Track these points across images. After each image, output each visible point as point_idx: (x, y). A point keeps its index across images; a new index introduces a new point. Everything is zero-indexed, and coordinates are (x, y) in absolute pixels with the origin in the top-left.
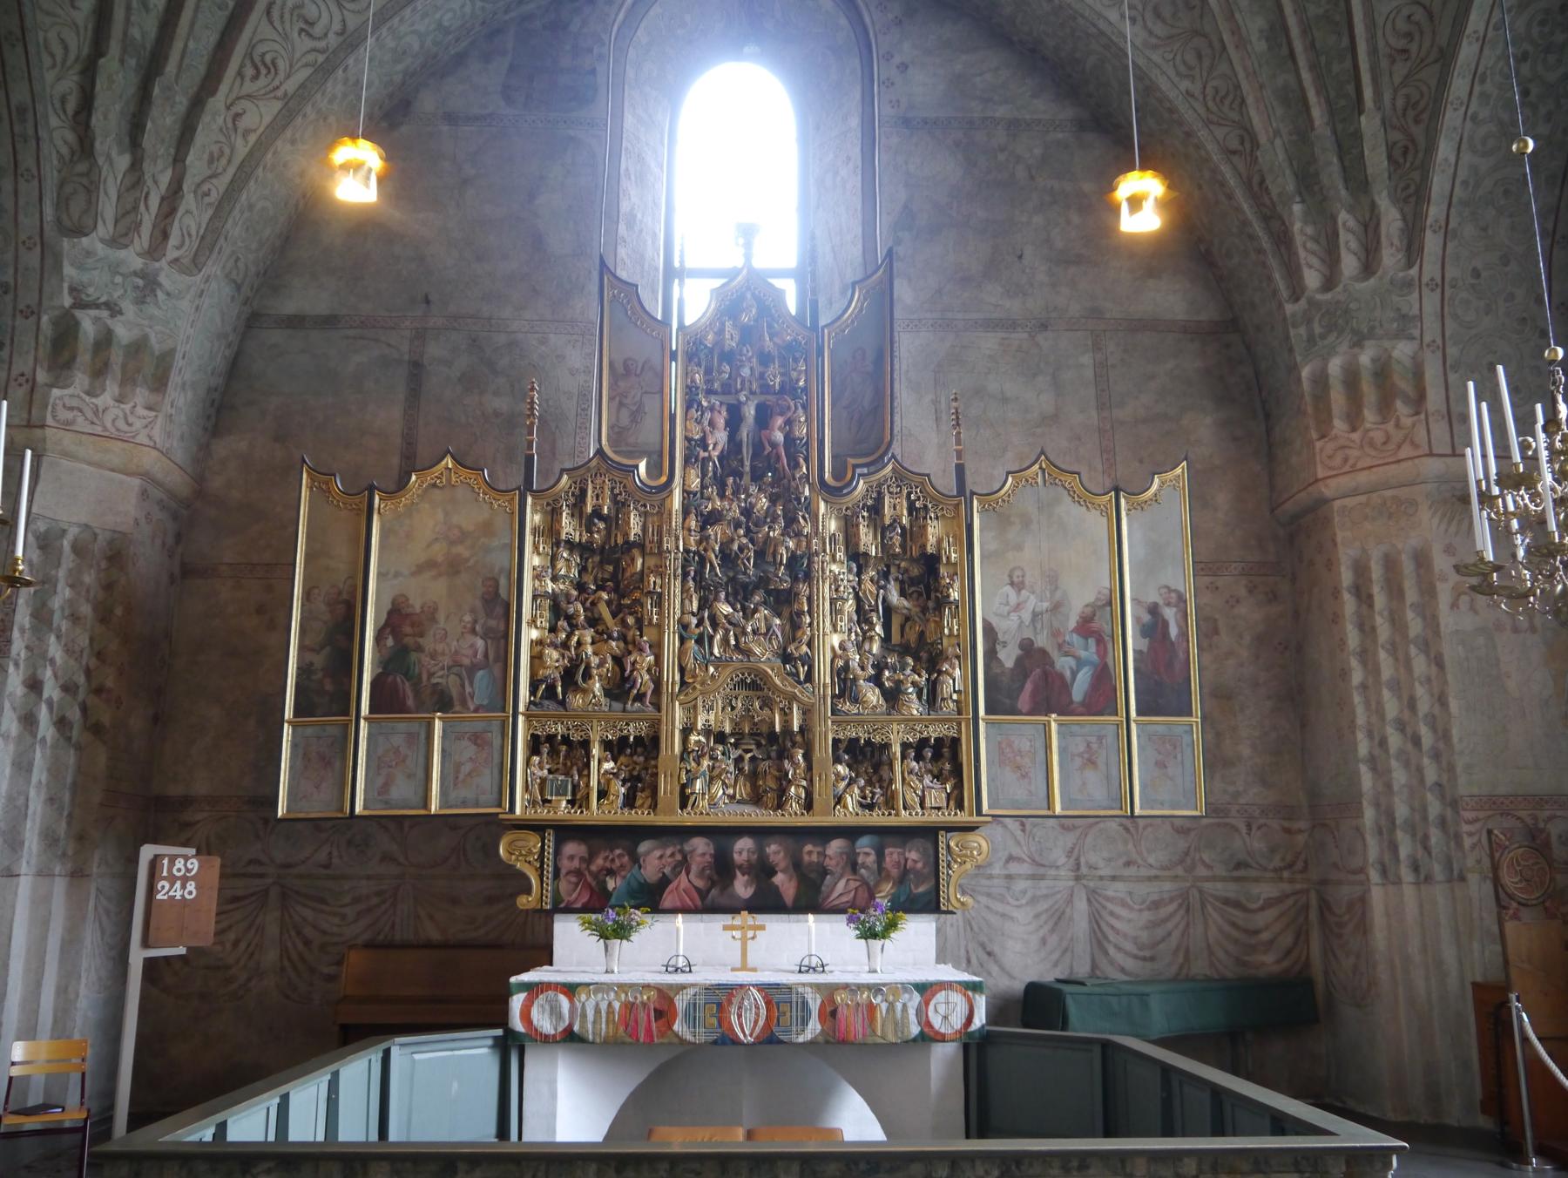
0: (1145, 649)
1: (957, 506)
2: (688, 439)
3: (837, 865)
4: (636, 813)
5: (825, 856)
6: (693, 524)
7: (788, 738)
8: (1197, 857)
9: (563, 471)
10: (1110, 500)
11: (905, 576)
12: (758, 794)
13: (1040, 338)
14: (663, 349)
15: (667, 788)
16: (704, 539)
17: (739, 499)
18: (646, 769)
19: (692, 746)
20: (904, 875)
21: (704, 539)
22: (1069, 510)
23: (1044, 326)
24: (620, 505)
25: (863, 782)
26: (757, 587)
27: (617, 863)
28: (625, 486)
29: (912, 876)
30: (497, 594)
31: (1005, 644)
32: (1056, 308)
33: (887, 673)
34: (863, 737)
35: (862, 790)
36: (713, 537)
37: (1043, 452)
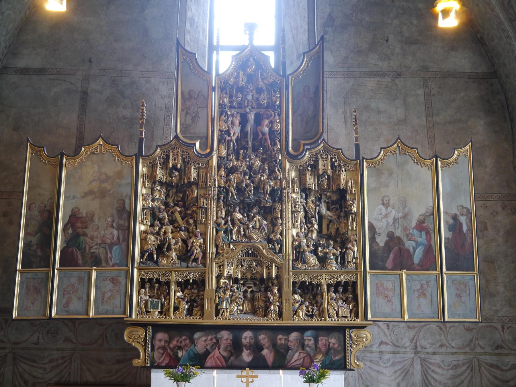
0: (450, 237)
1: (356, 165)
2: (220, 131)
3: (295, 345)
4: (193, 318)
5: (288, 341)
6: (223, 173)
7: (270, 281)
8: (477, 342)
9: (158, 146)
10: (433, 162)
11: (329, 200)
12: (255, 309)
13: (397, 81)
14: (208, 86)
15: (209, 306)
16: (228, 181)
17: (246, 161)
18: (198, 296)
19: (221, 285)
20: (329, 350)
21: (228, 181)
22: (412, 167)
23: (399, 75)
24: (186, 163)
25: (308, 303)
26: (255, 205)
27: (184, 343)
28: (189, 154)
29: (332, 351)
30: (124, 208)
31: (379, 235)
32: (405, 66)
33: (320, 249)
34: (308, 281)
35: (307, 307)
36: (233, 180)
37: (399, 138)
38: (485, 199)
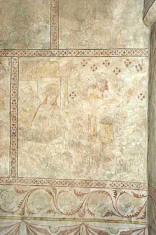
8: (86, 208)
38: (108, 55)
